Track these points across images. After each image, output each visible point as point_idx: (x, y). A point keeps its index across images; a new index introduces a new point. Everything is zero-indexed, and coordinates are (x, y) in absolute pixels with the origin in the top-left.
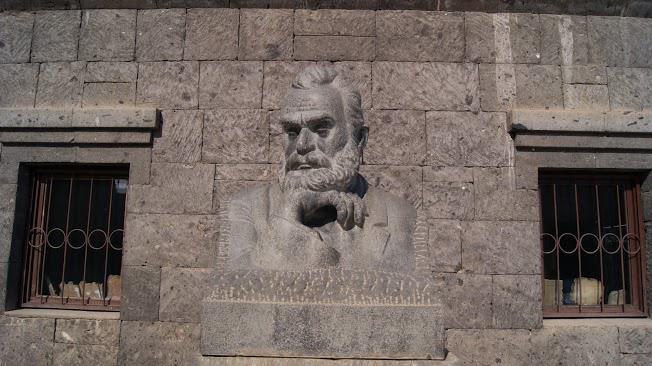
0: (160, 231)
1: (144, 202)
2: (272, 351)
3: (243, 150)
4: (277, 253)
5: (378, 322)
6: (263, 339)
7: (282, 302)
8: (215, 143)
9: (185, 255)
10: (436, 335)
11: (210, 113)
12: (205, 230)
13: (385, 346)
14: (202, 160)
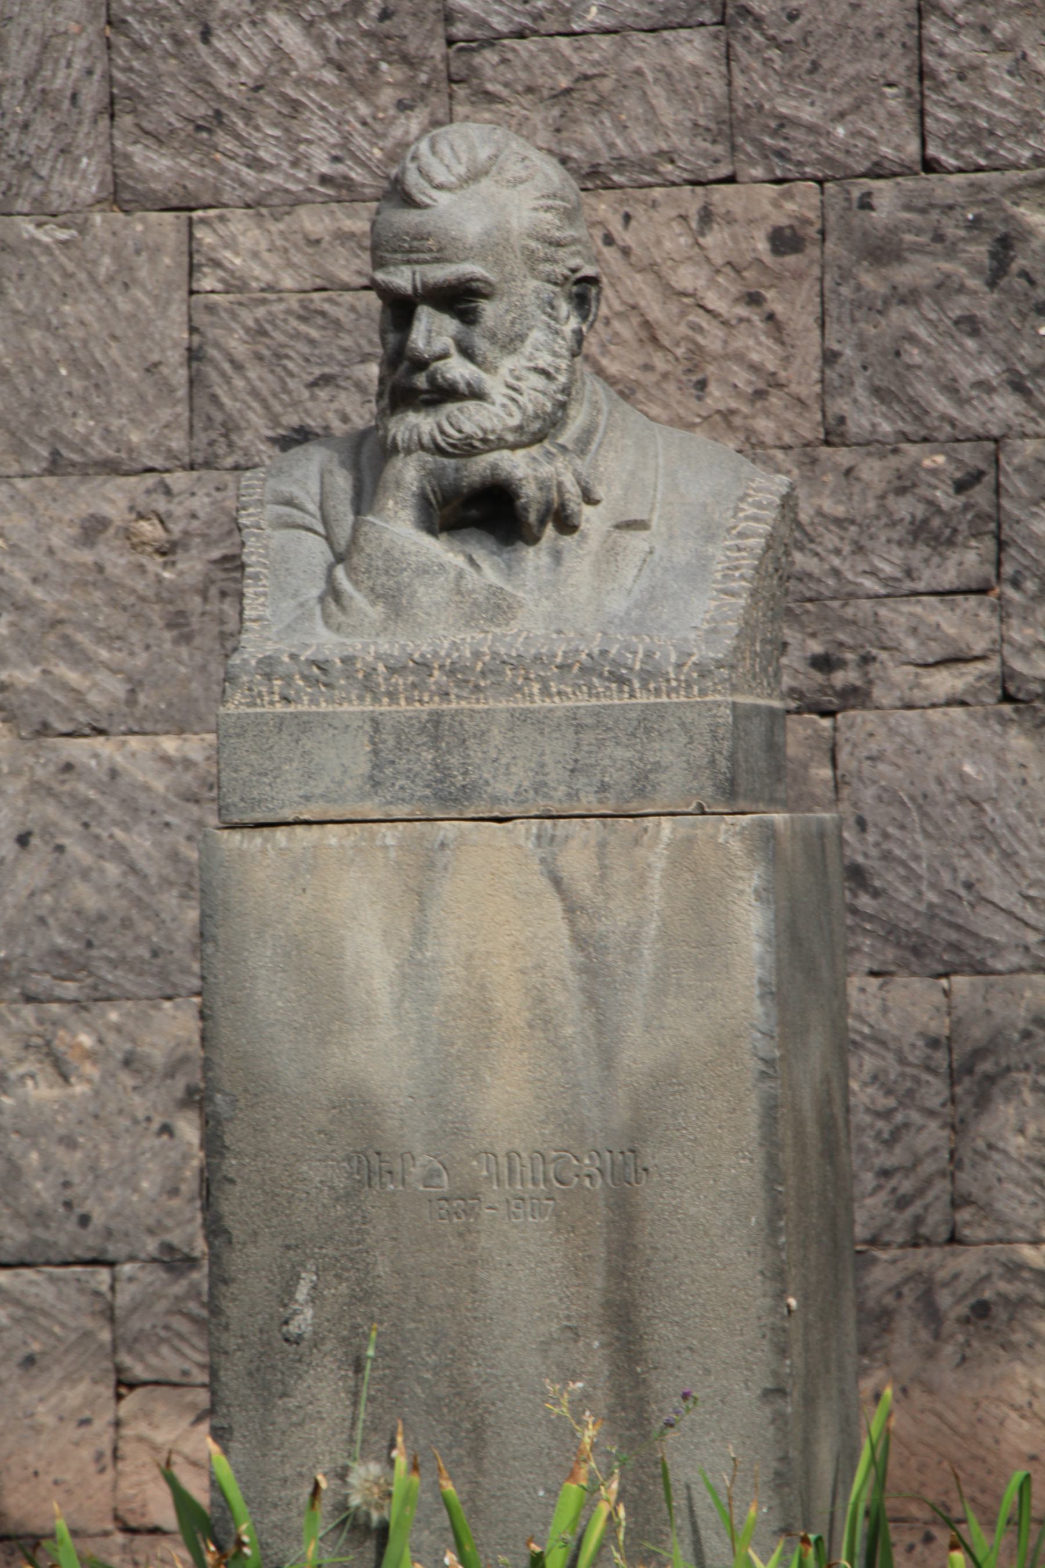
2: (370, 808)
3: (320, 131)
6: (349, 784)
7: (384, 706)
8: (176, 104)
9: (72, 677)
12: (166, 551)
14: (122, 194)
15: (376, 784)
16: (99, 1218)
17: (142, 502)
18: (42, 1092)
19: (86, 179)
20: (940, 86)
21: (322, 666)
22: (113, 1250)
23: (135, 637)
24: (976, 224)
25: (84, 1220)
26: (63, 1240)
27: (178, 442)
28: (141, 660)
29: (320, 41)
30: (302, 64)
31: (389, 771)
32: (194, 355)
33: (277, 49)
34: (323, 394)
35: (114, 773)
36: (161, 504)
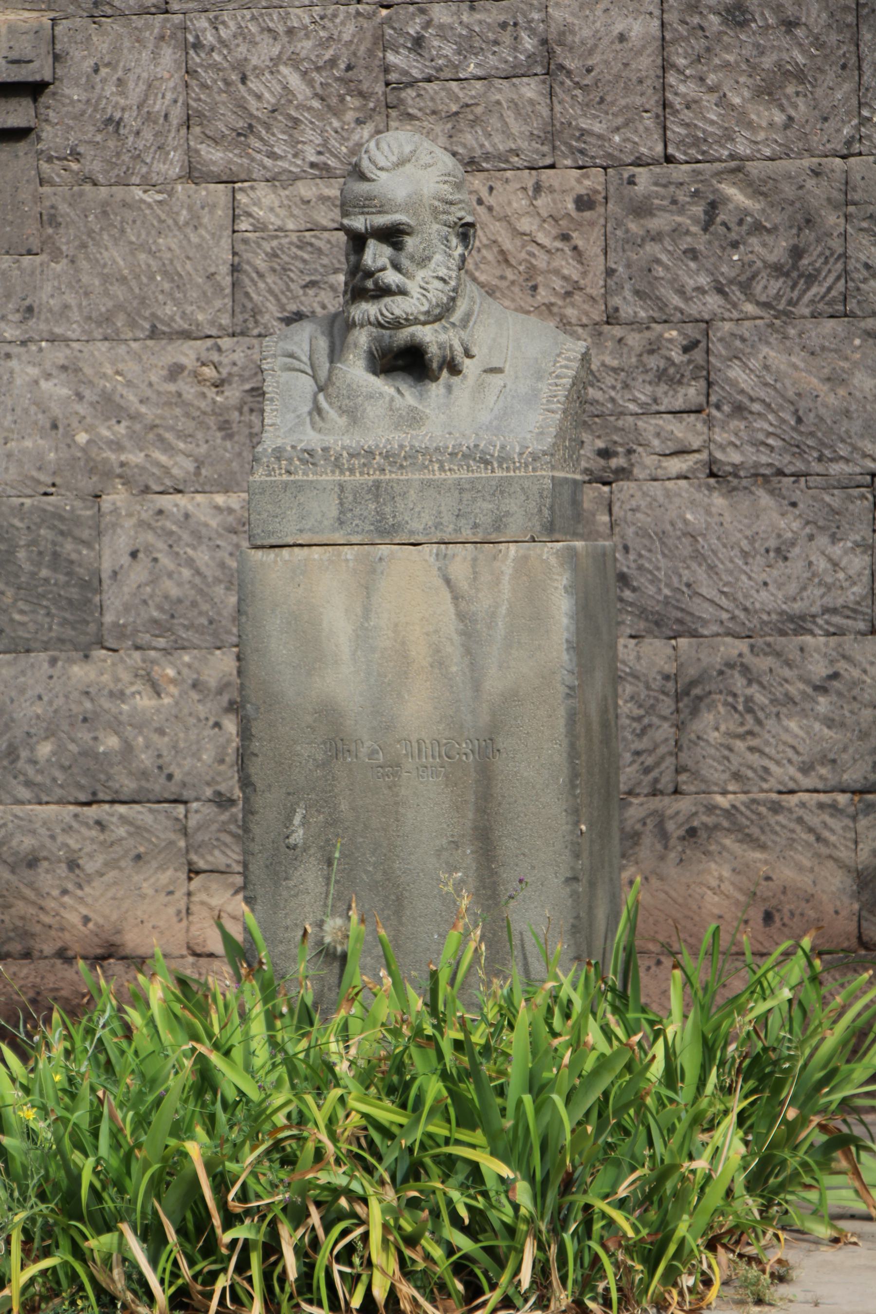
0: (87, 393)
1: (30, 309)
2: (338, 537)
4: (340, 416)
5: (466, 496)
6: (326, 523)
8: (226, 120)
9: (163, 458)
10: (540, 511)
11: (202, 23)
12: (218, 385)
13: (476, 526)
14: (193, 174)
15: (341, 523)
16: (178, 776)
17: (204, 356)
18: (145, 702)
19: (171, 165)
20: (676, 112)
21: (310, 453)
22: (186, 794)
23: (200, 435)
24: (696, 194)
25: (170, 777)
26: (157, 788)
27: (225, 320)
28: (203, 449)
29: (311, 83)
30: (300, 97)
31: (349, 515)
32: (235, 269)
33: (285, 88)
34: (311, 292)
35: (187, 516)
36: (215, 357)
